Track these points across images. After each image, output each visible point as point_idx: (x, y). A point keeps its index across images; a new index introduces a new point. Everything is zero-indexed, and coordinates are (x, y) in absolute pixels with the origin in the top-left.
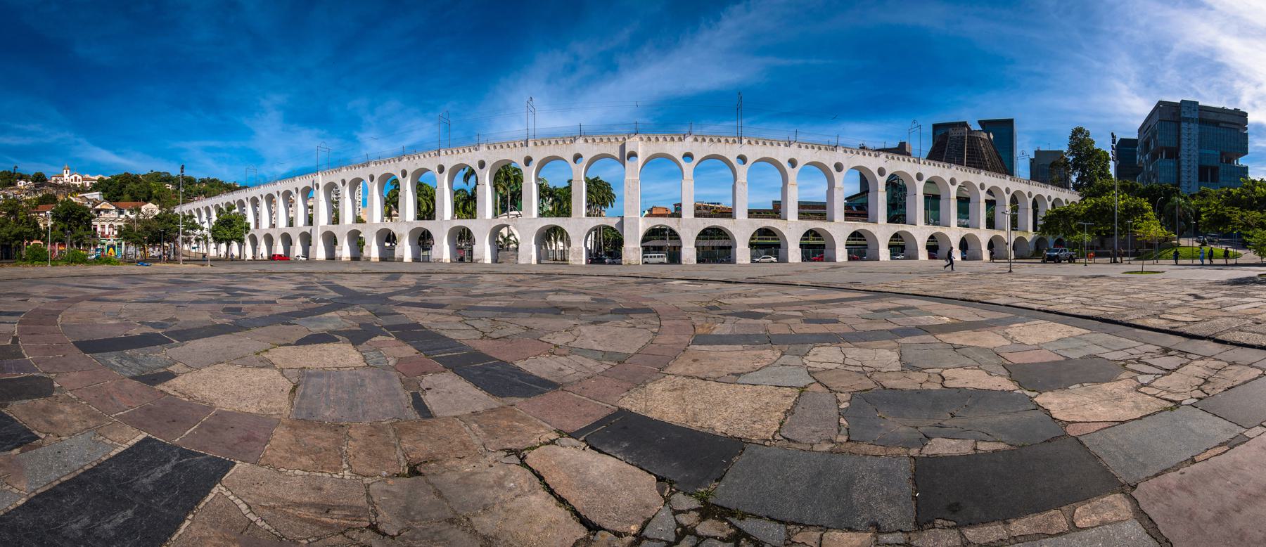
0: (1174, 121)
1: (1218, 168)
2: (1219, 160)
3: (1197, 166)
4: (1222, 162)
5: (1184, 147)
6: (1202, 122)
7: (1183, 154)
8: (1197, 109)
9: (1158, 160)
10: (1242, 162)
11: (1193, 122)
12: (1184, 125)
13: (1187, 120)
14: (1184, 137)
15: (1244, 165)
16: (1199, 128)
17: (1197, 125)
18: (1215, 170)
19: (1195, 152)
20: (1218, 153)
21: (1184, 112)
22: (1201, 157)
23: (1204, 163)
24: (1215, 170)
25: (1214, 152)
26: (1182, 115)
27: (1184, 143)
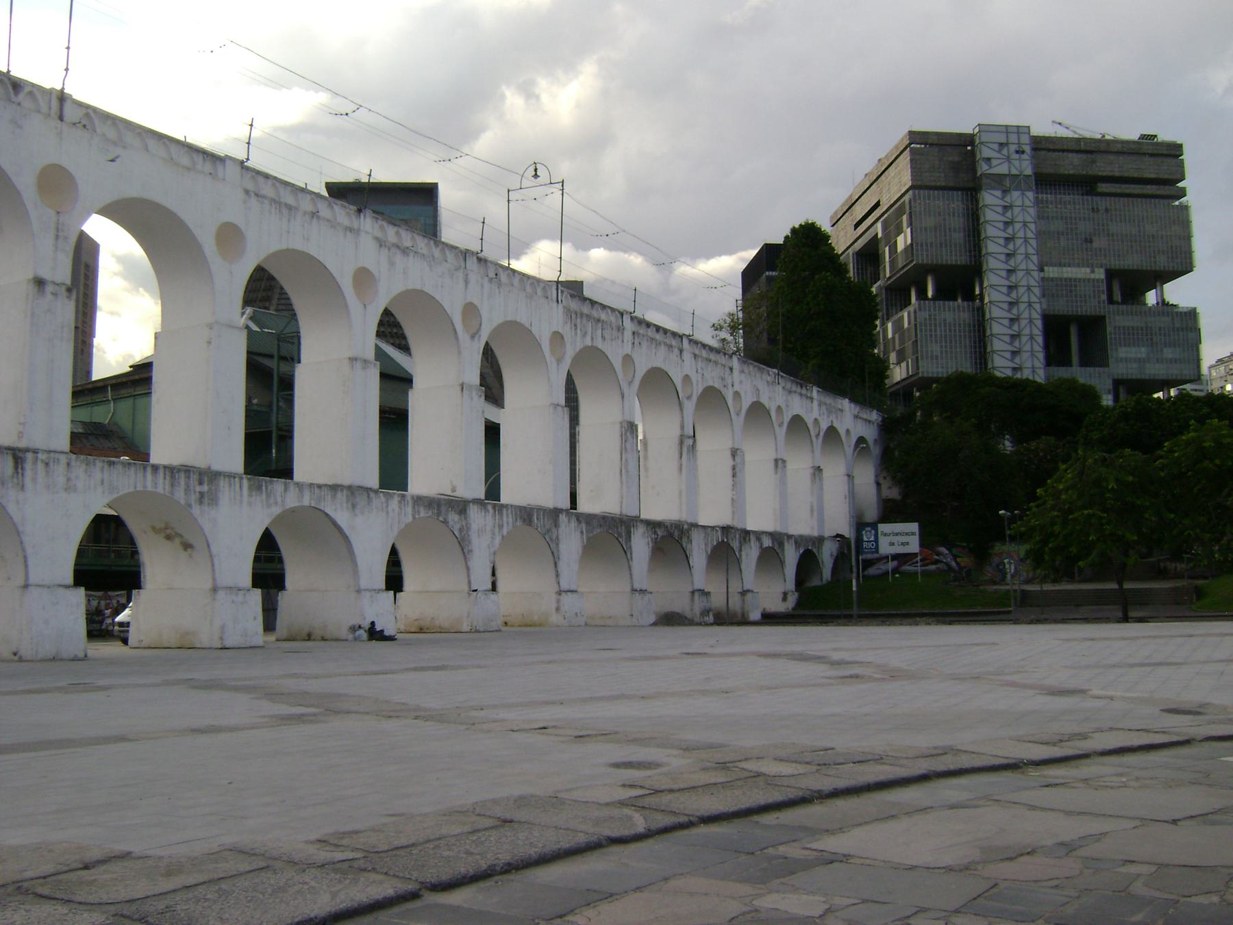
2: (1104, 297)
3: (1036, 316)
4: (1111, 300)
5: (994, 264)
6: (1045, 181)
7: (993, 288)
8: (1027, 149)
9: (911, 308)
10: (1177, 292)
12: (990, 198)
13: (999, 181)
14: (992, 232)
16: (1037, 202)
17: (1030, 195)
18: (1092, 327)
19: (1029, 279)
20: (1100, 274)
21: (989, 159)
22: (1049, 288)
24: (1092, 327)
25: (1082, 272)
26: (983, 168)
27: (993, 247)
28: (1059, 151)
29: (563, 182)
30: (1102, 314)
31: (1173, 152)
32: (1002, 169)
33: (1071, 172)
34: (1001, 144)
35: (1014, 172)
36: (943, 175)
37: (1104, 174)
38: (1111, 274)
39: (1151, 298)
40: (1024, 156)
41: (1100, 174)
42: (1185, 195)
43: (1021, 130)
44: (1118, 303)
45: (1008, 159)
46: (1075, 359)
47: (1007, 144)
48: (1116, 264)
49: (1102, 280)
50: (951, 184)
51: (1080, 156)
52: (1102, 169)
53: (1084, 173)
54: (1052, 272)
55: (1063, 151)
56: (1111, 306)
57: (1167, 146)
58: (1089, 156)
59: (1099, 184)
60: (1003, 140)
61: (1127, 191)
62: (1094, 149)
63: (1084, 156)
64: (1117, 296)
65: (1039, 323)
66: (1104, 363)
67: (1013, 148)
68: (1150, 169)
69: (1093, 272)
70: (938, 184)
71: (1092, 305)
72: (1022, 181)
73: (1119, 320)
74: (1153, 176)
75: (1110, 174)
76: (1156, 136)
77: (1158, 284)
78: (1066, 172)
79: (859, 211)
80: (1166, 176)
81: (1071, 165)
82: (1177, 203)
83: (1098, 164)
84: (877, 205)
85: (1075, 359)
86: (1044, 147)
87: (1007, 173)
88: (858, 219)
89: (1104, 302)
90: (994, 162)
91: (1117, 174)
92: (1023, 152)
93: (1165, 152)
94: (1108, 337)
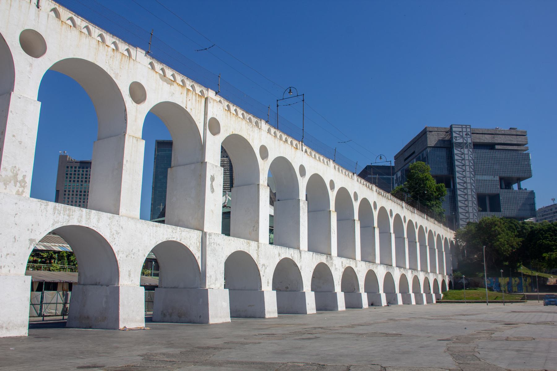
0: (445, 148)
1: (497, 196)
2: (499, 187)
4: (501, 188)
10: (526, 185)
11: (467, 147)
13: (460, 145)
15: (529, 189)
20: (497, 178)
21: (456, 137)
23: (482, 191)
28: (481, 134)
29: (391, 161)
30: (498, 193)
31: (523, 134)
32: (461, 141)
33: (486, 141)
34: (460, 132)
35: (465, 142)
36: (439, 142)
37: (498, 142)
38: (501, 179)
39: (515, 187)
40: (468, 136)
41: (496, 142)
42: (528, 150)
43: (468, 127)
44: (504, 189)
45: (462, 137)
46: (488, 209)
47: (462, 131)
48: (503, 175)
49: (498, 180)
50: (442, 146)
51: (489, 135)
52: (497, 140)
53: (491, 142)
54: (479, 177)
55: (482, 134)
56: (502, 190)
57: (521, 132)
58: (492, 135)
59: (496, 146)
60: (461, 131)
61: (506, 148)
62: (493, 133)
63: (490, 136)
64: (504, 186)
65: (475, 196)
66: (500, 211)
67: (464, 133)
68: (514, 140)
69: (494, 177)
70: (437, 146)
71: (495, 189)
72: (468, 145)
73: (504, 195)
74: (516, 143)
75: (500, 142)
76: (517, 128)
77: (518, 182)
78: (484, 141)
79: (407, 154)
80: (521, 143)
81: (487, 139)
82: (525, 152)
83: (496, 139)
84: (414, 153)
85: (488, 209)
86: (475, 132)
87: (462, 142)
88: (406, 157)
89: (499, 188)
90: (458, 138)
91: (502, 142)
92: (468, 134)
93: (520, 134)
94: (501, 201)
